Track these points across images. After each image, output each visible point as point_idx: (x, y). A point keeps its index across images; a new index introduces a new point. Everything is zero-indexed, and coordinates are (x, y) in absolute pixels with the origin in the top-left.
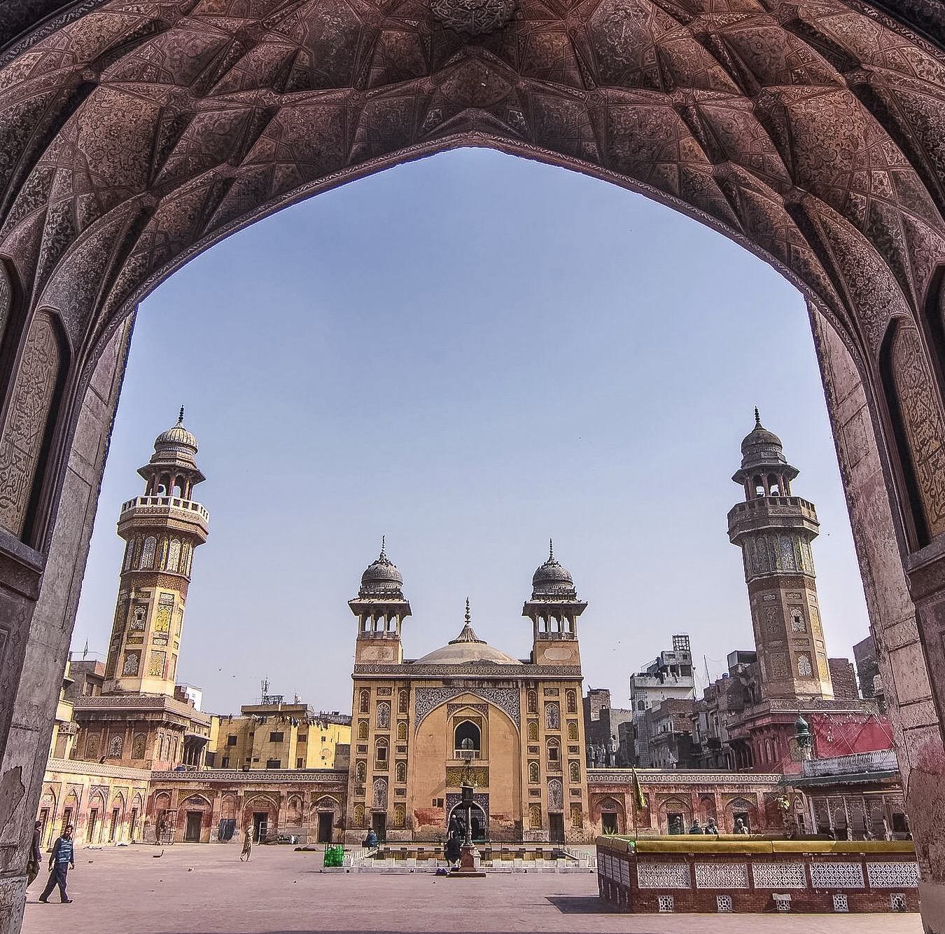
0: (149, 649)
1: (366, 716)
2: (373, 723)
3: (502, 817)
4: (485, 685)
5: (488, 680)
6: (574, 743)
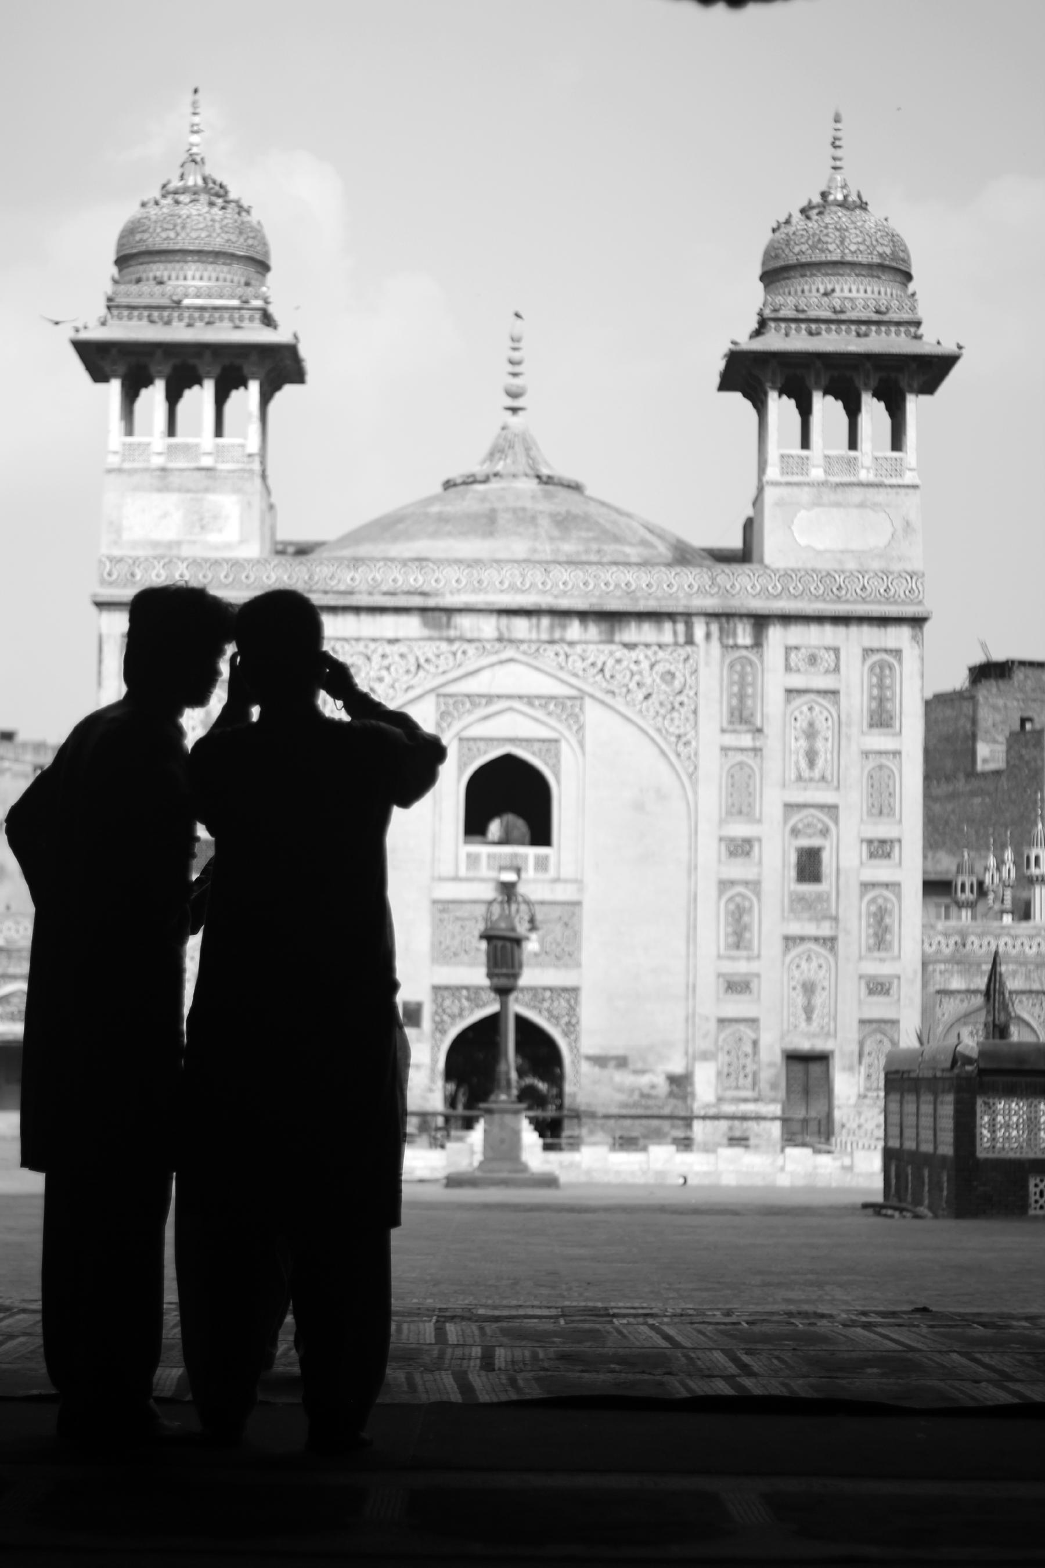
3: (622, 1062)
4: (574, 629)
5: (583, 616)
6: (882, 830)
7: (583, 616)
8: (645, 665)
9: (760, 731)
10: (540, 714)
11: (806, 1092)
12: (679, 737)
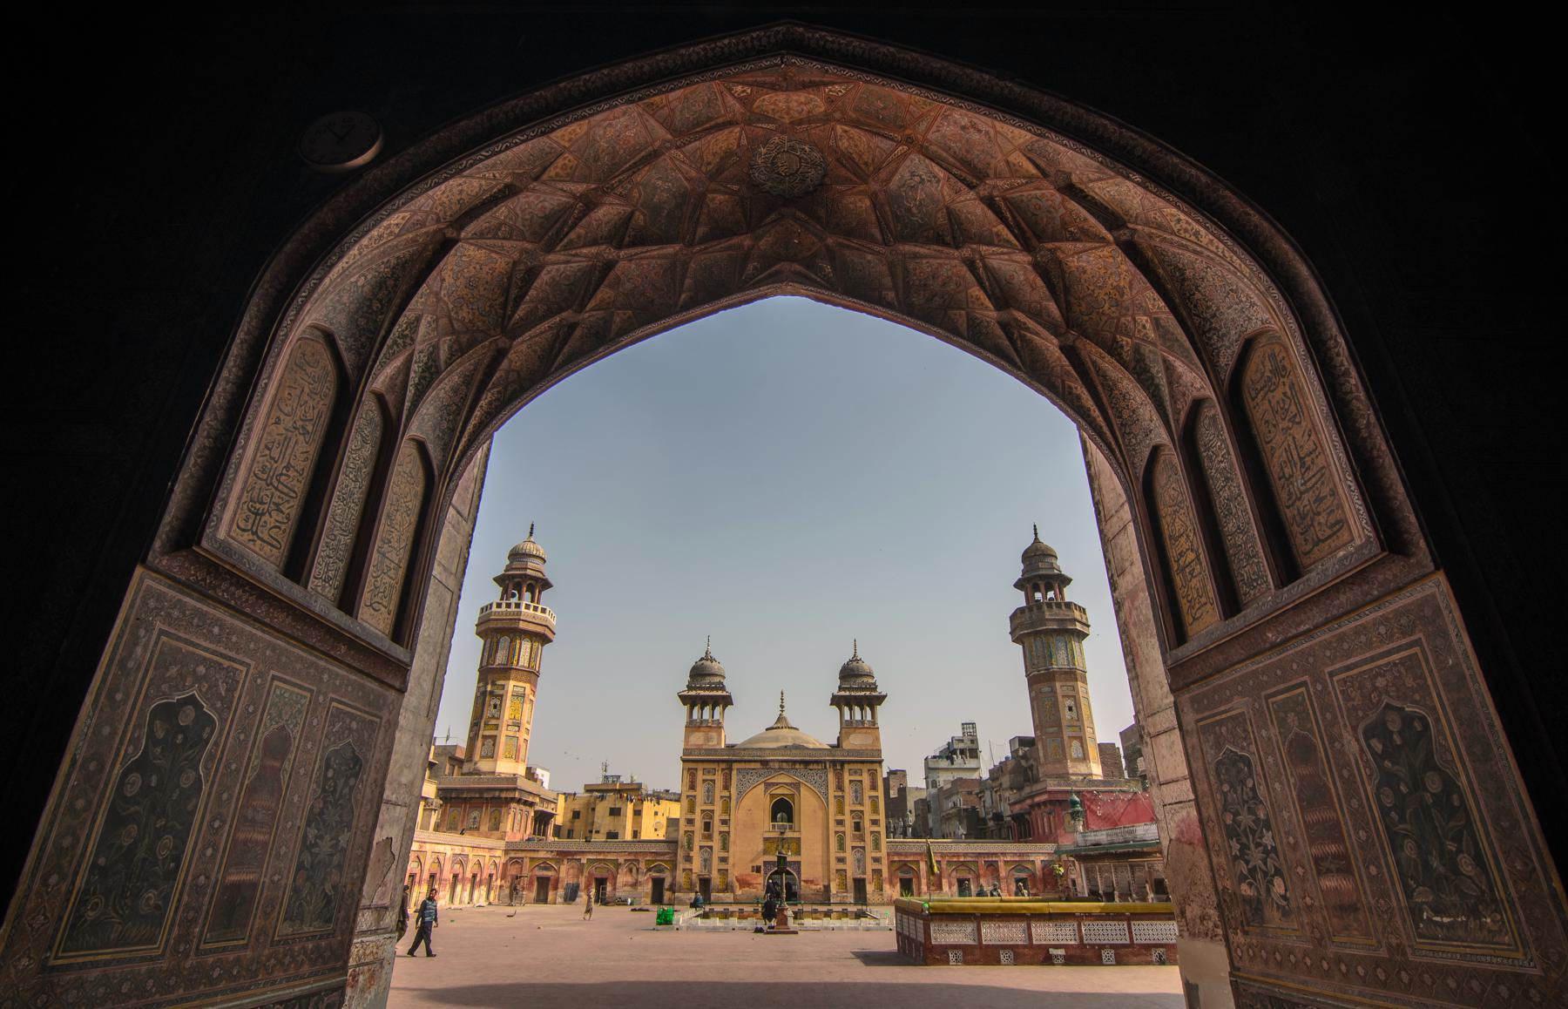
0: (504, 734)
1: (694, 793)
4: (797, 766)
6: (875, 817)
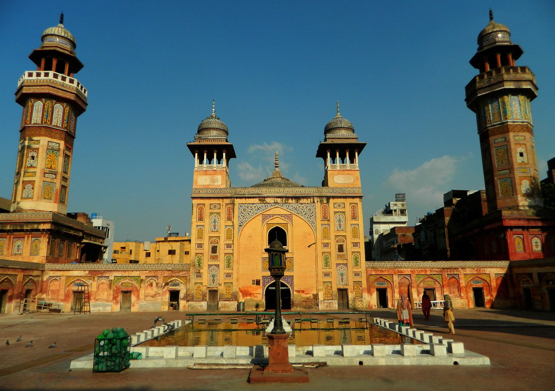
2: (207, 229)
3: (303, 292)
4: (290, 201)
5: (292, 198)
6: (356, 240)
7: (292, 198)
8: (305, 207)
9: (329, 220)
10: (283, 218)
11: (343, 297)
12: (312, 222)
